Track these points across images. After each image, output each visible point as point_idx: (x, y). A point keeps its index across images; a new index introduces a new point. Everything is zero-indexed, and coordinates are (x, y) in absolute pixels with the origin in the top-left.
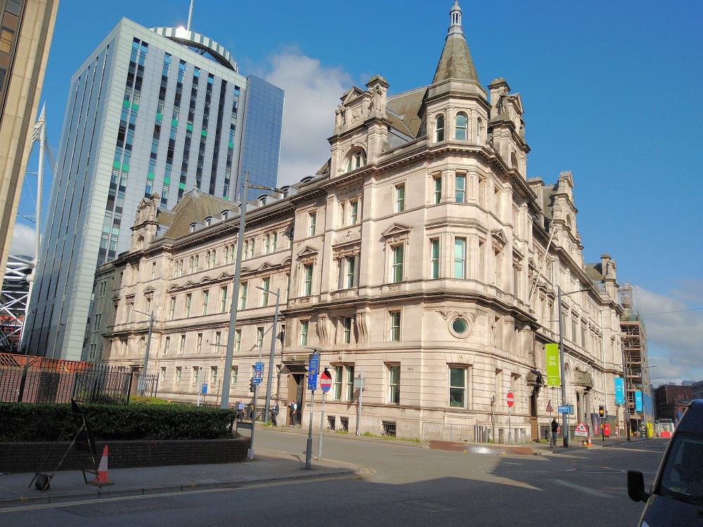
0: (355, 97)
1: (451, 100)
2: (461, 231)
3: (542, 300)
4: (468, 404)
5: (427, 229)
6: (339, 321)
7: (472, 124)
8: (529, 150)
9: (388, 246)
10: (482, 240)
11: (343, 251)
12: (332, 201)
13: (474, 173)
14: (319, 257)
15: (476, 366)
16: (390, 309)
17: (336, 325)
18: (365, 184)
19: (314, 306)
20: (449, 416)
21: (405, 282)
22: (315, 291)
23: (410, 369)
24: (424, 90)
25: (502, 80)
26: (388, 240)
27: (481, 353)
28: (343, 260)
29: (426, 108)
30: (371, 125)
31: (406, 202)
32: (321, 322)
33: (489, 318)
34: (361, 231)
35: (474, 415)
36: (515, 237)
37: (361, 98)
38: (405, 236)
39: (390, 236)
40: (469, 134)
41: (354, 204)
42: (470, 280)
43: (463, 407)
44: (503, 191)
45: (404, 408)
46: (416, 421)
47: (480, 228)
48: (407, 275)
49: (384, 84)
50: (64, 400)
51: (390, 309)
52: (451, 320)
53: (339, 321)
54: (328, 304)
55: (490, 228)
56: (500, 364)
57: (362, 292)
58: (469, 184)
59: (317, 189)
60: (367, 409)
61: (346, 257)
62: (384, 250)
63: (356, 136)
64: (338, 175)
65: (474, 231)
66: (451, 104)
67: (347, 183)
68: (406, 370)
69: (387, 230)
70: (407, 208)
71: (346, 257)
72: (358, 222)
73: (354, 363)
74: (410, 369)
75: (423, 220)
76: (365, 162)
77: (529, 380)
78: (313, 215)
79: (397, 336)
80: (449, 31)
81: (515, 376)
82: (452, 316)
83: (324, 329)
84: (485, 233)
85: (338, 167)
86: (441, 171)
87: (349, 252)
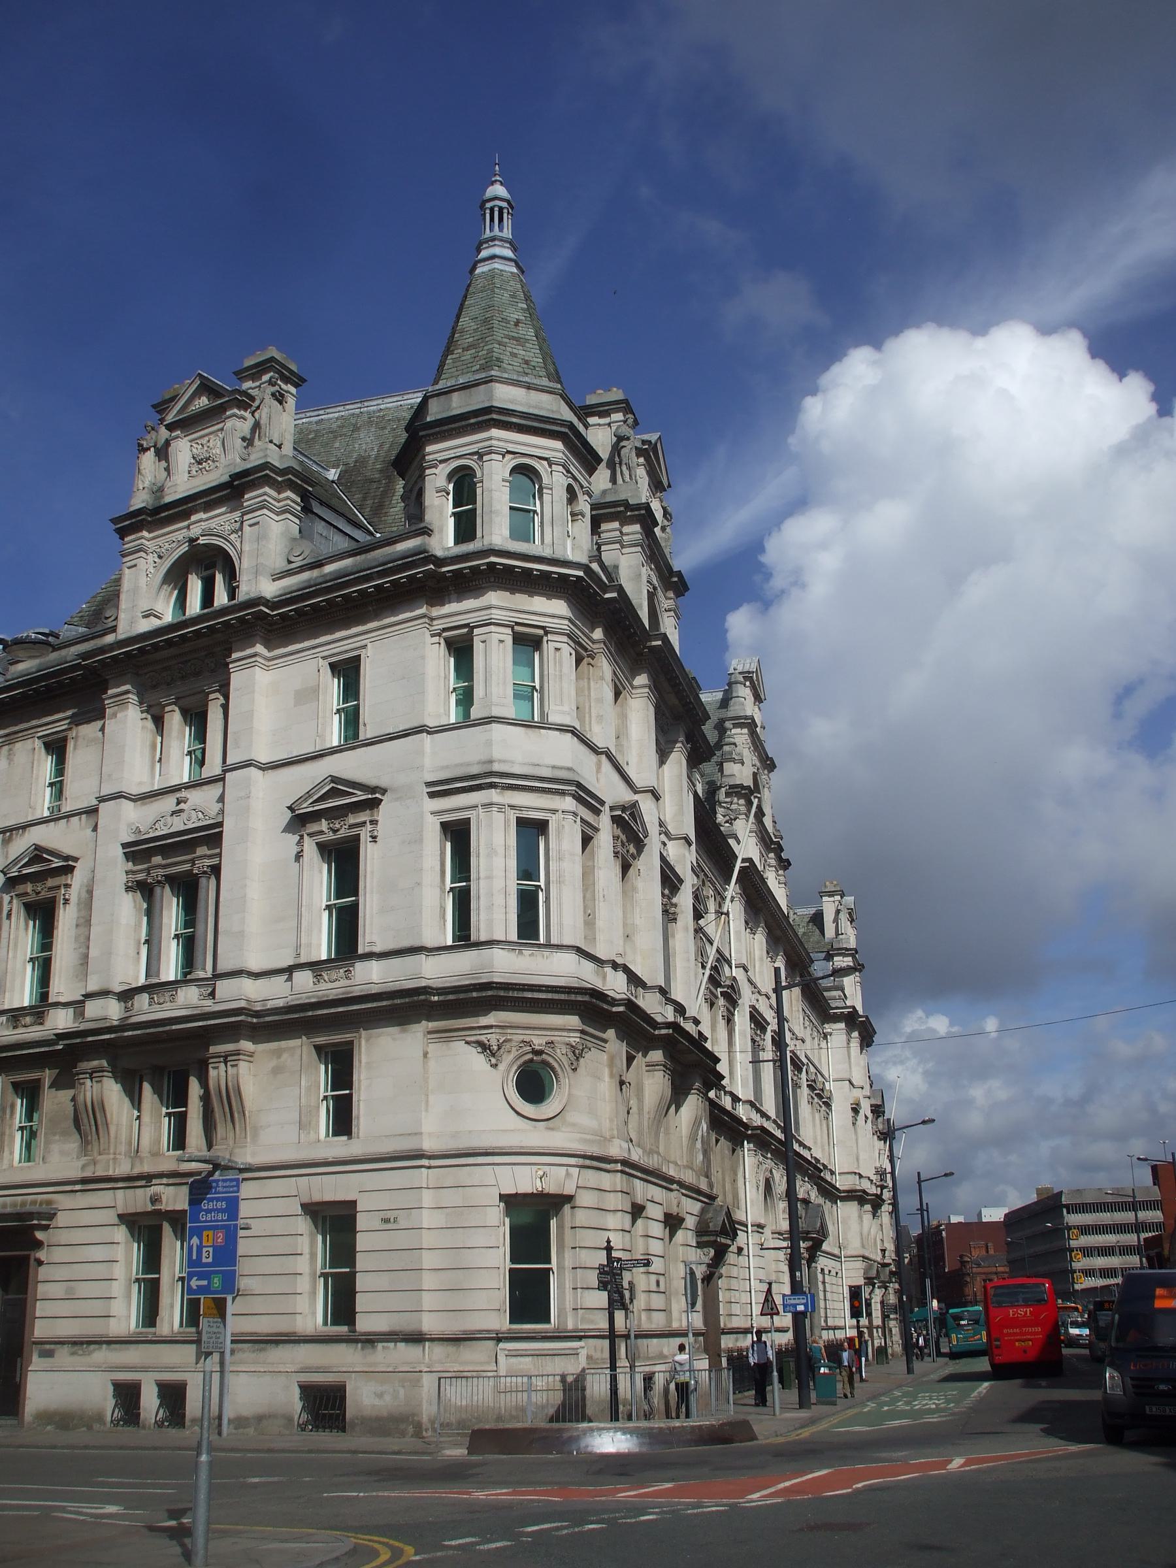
0: (203, 402)
1: (495, 432)
2: (533, 804)
3: (712, 1005)
4: (562, 1311)
5: (432, 795)
6: (147, 1088)
7: (553, 501)
8: (686, 588)
9: (310, 847)
10: (590, 832)
11: (157, 860)
12: (123, 704)
13: (565, 639)
14: (78, 880)
15: (584, 1199)
16: (321, 1040)
17: (136, 1100)
18: (235, 656)
19: (60, 1037)
20: (512, 1354)
21: (370, 956)
22: (63, 987)
23: (386, 1221)
24: (416, 398)
25: (616, 394)
26: (313, 827)
27: (598, 1162)
28: (158, 890)
29: (421, 448)
30: (254, 485)
31: (365, 715)
32: (89, 1090)
33: (612, 1059)
34: (221, 799)
35: (582, 1343)
36: (664, 831)
37: (222, 409)
38: (363, 817)
39: (315, 816)
40: (548, 529)
41: (197, 719)
42: (559, 947)
43: (548, 1321)
44: (631, 694)
45: (370, 1340)
46: (413, 1375)
47: (587, 798)
48: (371, 935)
49: (289, 377)
50: (383, 1282)
51: (321, 1040)
52: (511, 1065)
53: (147, 1088)
54: (110, 1029)
55: (609, 800)
56: (643, 1190)
57: (225, 988)
58: (551, 669)
59: (77, 667)
60: (247, 1354)
61: (171, 880)
62: (299, 857)
63: (202, 515)
64: (145, 626)
65: (569, 803)
66: (494, 442)
67: (173, 651)
68: (378, 1224)
69: (309, 794)
70: (365, 733)
71: (171, 880)
72: (213, 767)
73: (354, 1203)
74: (386, 1221)
75: (421, 768)
76: (232, 594)
77: (702, 1231)
78: (57, 748)
79: (343, 1122)
80: (479, 251)
81: (673, 1222)
82: (514, 1053)
83: (98, 1109)
84: (597, 812)
85: (144, 605)
86: (471, 628)
87: (180, 865)
